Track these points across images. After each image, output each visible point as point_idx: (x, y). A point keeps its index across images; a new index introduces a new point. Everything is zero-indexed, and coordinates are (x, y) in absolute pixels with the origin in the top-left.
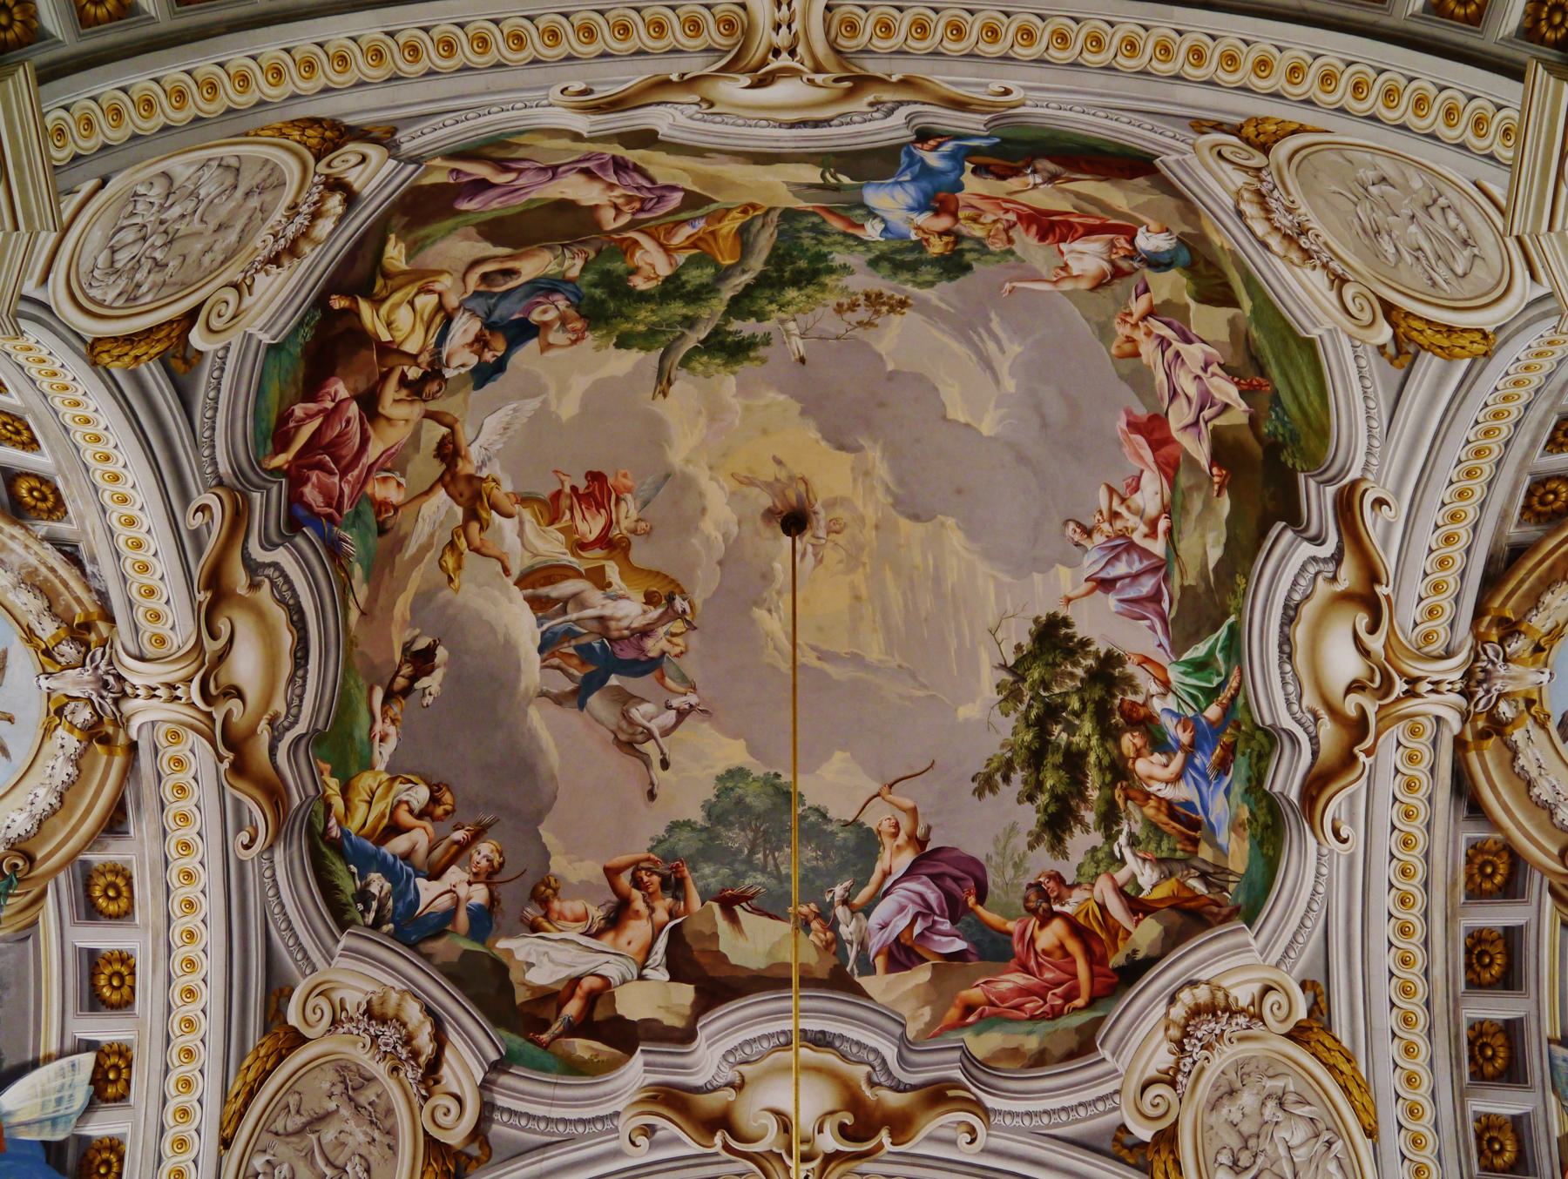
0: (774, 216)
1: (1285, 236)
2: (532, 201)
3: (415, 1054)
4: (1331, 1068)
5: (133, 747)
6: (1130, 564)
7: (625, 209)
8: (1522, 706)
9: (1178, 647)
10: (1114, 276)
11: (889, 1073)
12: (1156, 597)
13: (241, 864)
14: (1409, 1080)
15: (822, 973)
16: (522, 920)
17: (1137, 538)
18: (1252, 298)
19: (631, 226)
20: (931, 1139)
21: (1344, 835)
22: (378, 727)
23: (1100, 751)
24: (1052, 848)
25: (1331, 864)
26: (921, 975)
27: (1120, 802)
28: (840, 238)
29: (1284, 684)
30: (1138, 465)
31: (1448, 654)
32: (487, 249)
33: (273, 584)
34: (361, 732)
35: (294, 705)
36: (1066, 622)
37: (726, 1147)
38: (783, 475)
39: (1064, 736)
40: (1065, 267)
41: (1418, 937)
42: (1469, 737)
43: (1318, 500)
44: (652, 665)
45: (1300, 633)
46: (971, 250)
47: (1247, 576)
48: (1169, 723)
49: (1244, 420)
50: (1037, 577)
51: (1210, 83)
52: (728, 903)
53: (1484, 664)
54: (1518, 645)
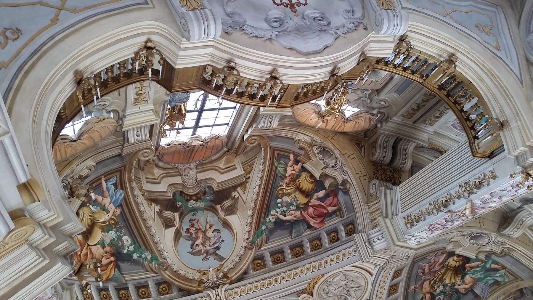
4: (314, 286)
8: (219, 272)
14: (308, 270)
31: (209, 295)
41: (277, 277)
53: (211, 285)
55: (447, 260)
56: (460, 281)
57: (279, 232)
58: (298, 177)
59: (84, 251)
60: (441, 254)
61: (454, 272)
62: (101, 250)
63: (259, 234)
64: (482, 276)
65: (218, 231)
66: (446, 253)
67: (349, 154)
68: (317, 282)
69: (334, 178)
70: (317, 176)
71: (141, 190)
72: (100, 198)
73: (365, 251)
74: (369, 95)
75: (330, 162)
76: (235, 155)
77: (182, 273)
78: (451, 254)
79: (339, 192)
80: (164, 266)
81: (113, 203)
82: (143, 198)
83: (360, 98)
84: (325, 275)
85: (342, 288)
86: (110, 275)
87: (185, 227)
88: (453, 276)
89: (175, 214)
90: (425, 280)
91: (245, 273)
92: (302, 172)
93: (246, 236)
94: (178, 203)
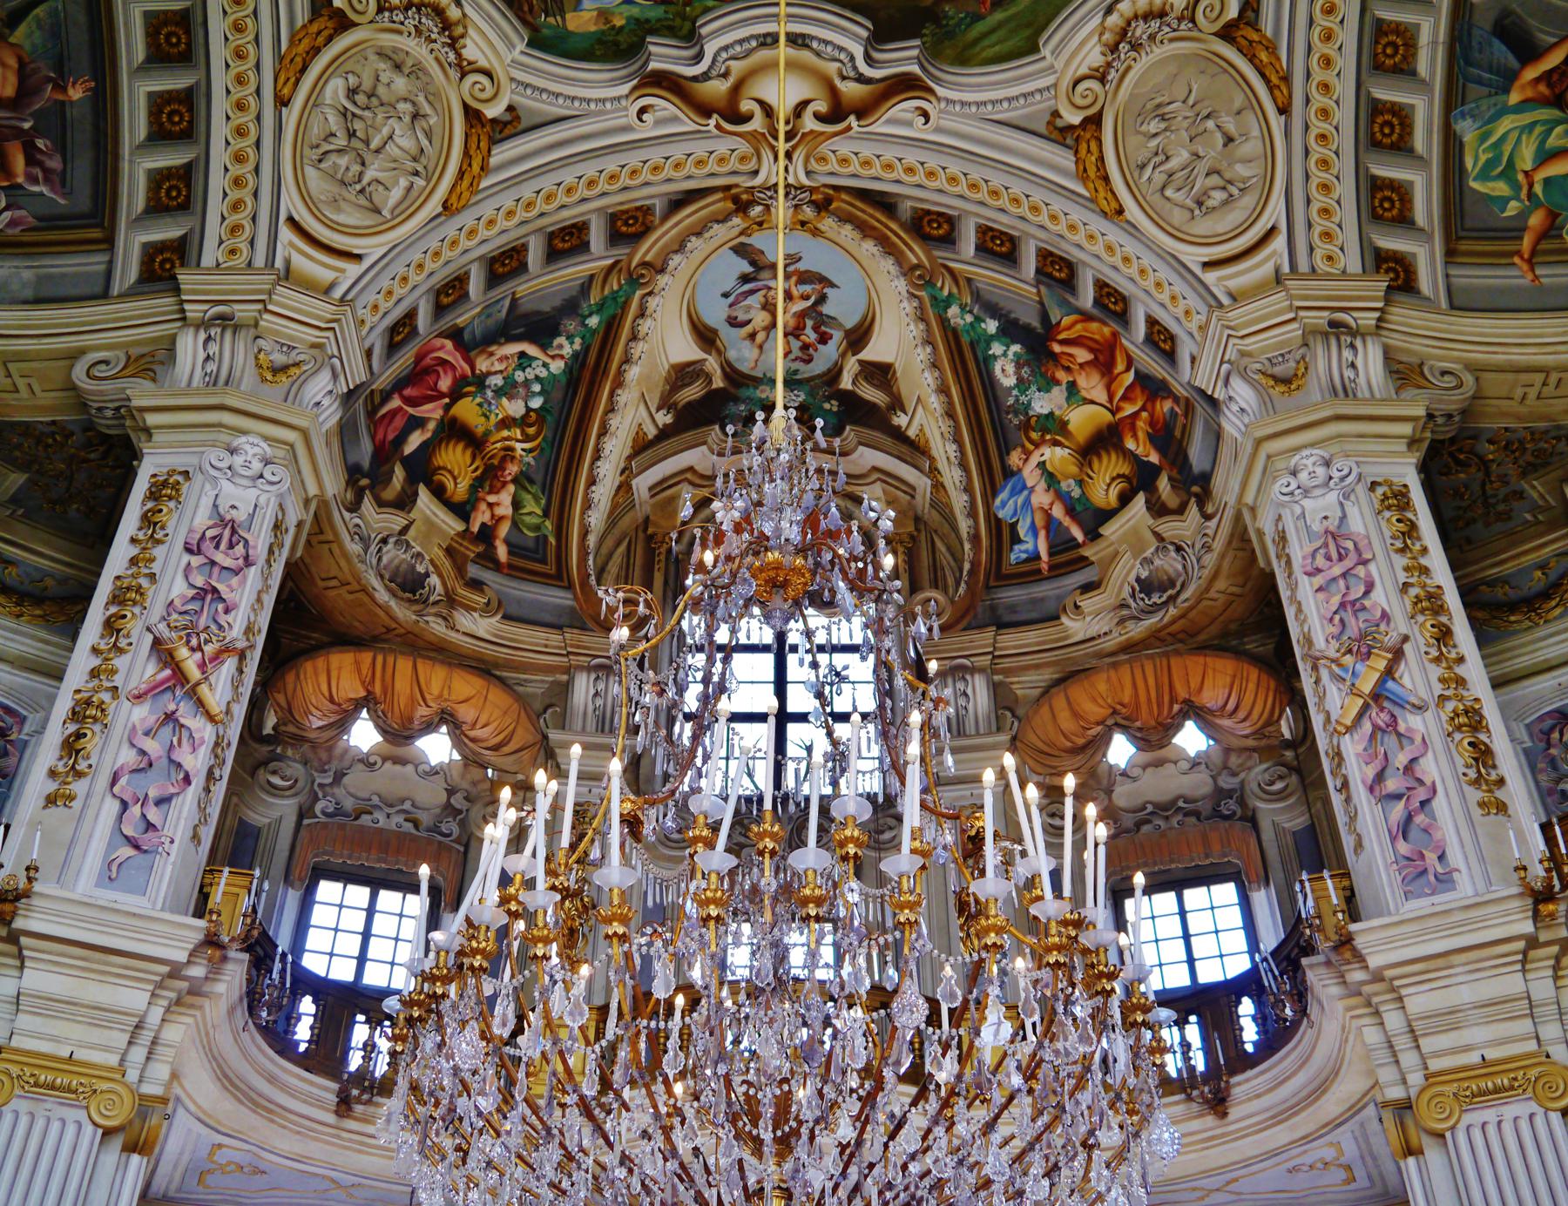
4: (466, 153)
21: (645, 117)
25: (613, 112)
29: (741, 42)
31: (808, 173)
42: (734, 191)
43: (904, 58)
51: (1311, 22)
54: (808, 212)
57: (546, 307)
58: (477, 485)
59: (1129, 409)
62: (1082, 382)
63: (609, 302)
65: (733, 322)
67: (343, 591)
68: (461, 174)
69: (381, 503)
70: (424, 497)
71: (938, 486)
72: (1058, 512)
73: (344, 340)
74: (316, 799)
75: (393, 553)
76: (650, 531)
77: (869, 246)
79: (371, 464)
81: (1024, 487)
82: (940, 466)
83: (339, 777)
84: (440, 209)
85: (373, 146)
89: (850, 387)
91: (678, 202)
92: (467, 502)
93: (652, 303)
94: (835, 409)
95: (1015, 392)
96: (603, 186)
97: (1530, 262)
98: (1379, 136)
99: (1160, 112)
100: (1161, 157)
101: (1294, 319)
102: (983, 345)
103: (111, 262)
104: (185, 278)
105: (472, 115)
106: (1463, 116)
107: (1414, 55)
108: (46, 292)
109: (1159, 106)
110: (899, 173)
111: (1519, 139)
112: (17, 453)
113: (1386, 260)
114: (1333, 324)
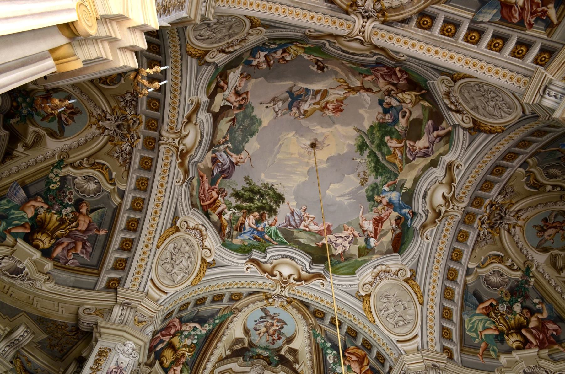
0: (397, 173)
1: (378, 274)
2: (424, 133)
3: (228, 48)
4: (200, 270)
5: (347, 13)
6: (297, 220)
7: (412, 147)
9: (280, 229)
10: (363, 230)
11: (192, 160)
12: (290, 225)
13: (306, 29)
15: (215, 142)
16: (244, 72)
17: (303, 222)
18: (362, 261)
19: (406, 145)
20: (178, 172)
21: (248, 270)
22: (313, 57)
23: (254, 207)
24: (232, 194)
26: (210, 165)
27: (242, 211)
28: (386, 181)
29: (277, 255)
30: (320, 225)
31: (288, 293)
32: (414, 116)
33: (367, 55)
34: (315, 54)
35: (335, 48)
36: (283, 202)
37: (184, 122)
38: (324, 145)
39: (257, 198)
40: (365, 220)
43: (319, 268)
44: (290, 108)
45: (288, 260)
46: (374, 204)
47: (298, 248)
48: (262, 225)
49: (334, 254)
50: (293, 197)
51: (430, 283)
52: (233, 120)
54: (285, 303)
55: (51, 246)
56: (39, 212)
60: (59, 259)
61: (45, 226)
62: (352, 365)
64: (13, 211)
66: (53, 257)
68: (197, 275)
70: (157, 363)
77: (300, 316)
78: (47, 253)
80: (312, 327)
85: (176, 263)
86: (354, 349)
87: (281, 342)
88: (48, 220)
89: (283, 354)
90: (84, 232)
91: (250, 294)
92: (168, 368)
93: (235, 319)
94: (277, 359)
95: (332, 365)
96: (233, 286)
97: (481, 356)
98: (444, 315)
99: (386, 297)
100: (386, 309)
101: (423, 362)
102: (325, 349)
103: (98, 280)
104: (119, 290)
105: (203, 260)
106: (465, 314)
107: (454, 296)
108: (75, 285)
109: (386, 295)
110: (313, 298)
111: (478, 323)
112: (48, 329)
113: (446, 349)
114: (434, 365)
